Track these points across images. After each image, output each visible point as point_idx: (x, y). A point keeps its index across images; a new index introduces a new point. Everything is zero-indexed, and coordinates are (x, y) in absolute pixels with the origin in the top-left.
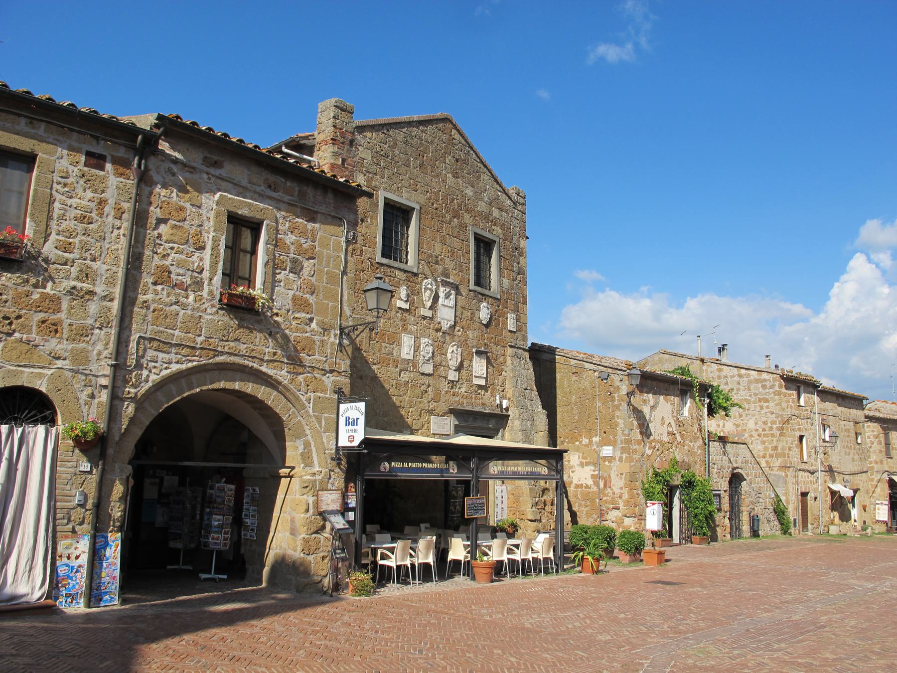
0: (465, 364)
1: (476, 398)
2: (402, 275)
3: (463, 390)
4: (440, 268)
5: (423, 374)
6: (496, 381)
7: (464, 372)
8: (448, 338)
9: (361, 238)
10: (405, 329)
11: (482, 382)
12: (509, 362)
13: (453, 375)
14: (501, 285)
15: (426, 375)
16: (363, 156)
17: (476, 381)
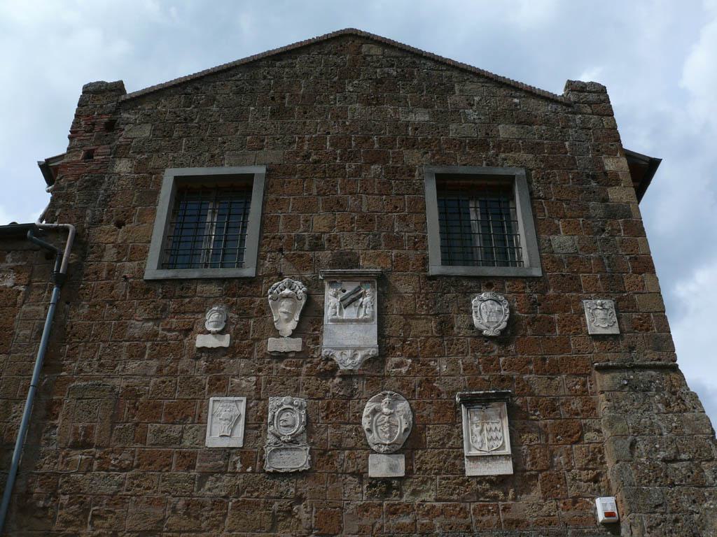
0: (431, 434)
1: (481, 511)
2: (214, 289)
3: (429, 497)
4: (325, 255)
5: (275, 474)
6: (560, 459)
7: (429, 457)
8: (359, 385)
9: (115, 250)
10: (220, 386)
11: (506, 468)
12: (603, 405)
13: (379, 467)
14: (546, 254)
15: (287, 475)
16: (131, 134)
17: (472, 470)
